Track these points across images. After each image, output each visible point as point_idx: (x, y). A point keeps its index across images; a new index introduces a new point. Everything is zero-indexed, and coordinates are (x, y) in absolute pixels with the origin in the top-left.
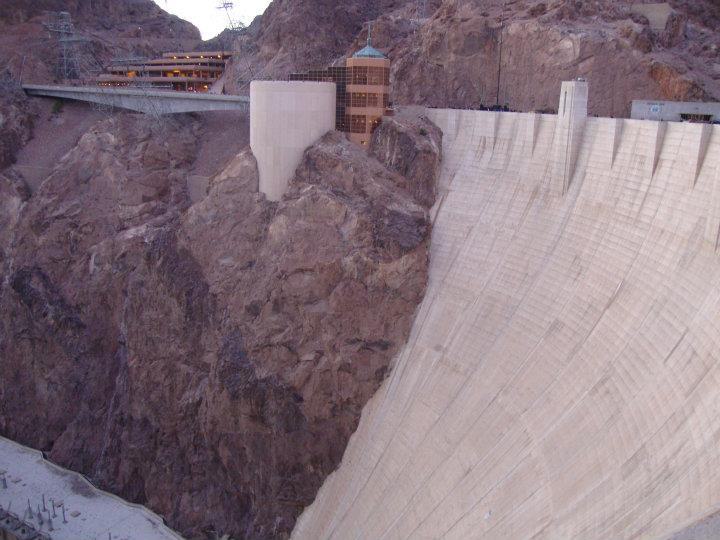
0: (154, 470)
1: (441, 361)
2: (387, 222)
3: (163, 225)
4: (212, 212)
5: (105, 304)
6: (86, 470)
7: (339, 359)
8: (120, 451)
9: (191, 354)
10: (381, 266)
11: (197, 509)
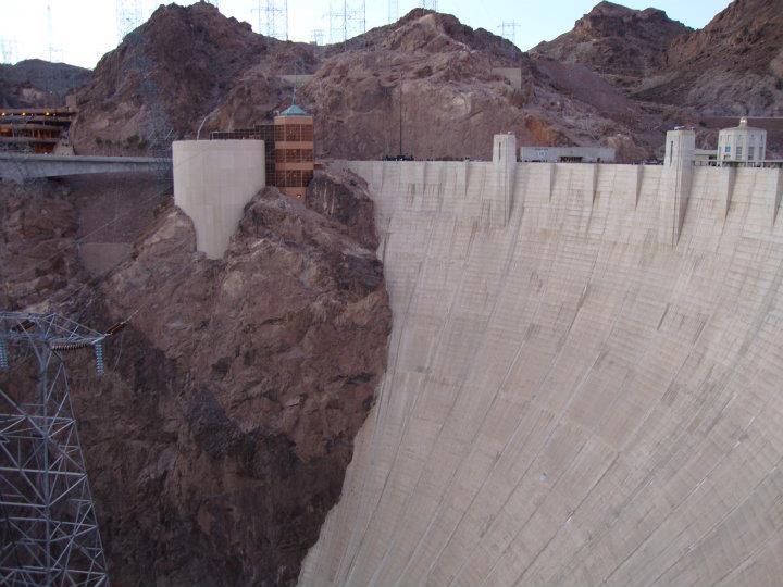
1: (427, 379)
2: (346, 266)
3: (68, 299)
4: (146, 276)
7: (325, 397)
10: (350, 306)
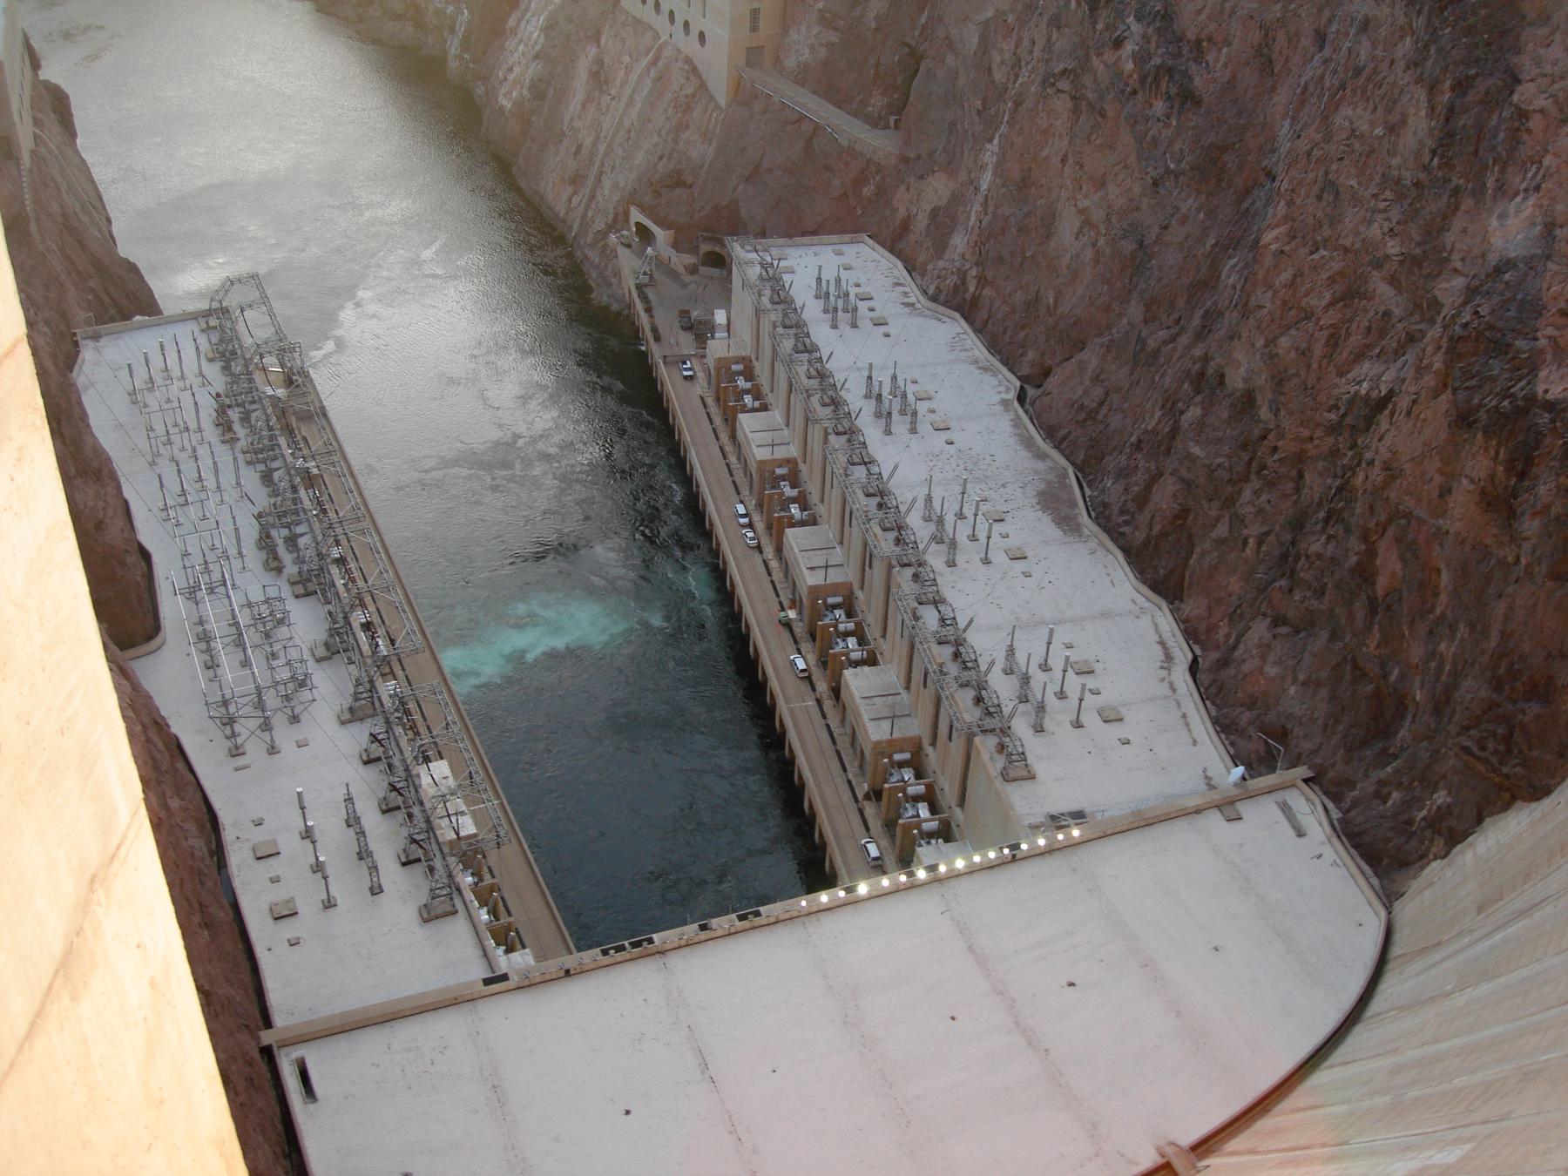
0: (1222, 530)
5: (1265, 62)
6: (1088, 470)
8: (1169, 452)
9: (1412, 262)
11: (1271, 671)
